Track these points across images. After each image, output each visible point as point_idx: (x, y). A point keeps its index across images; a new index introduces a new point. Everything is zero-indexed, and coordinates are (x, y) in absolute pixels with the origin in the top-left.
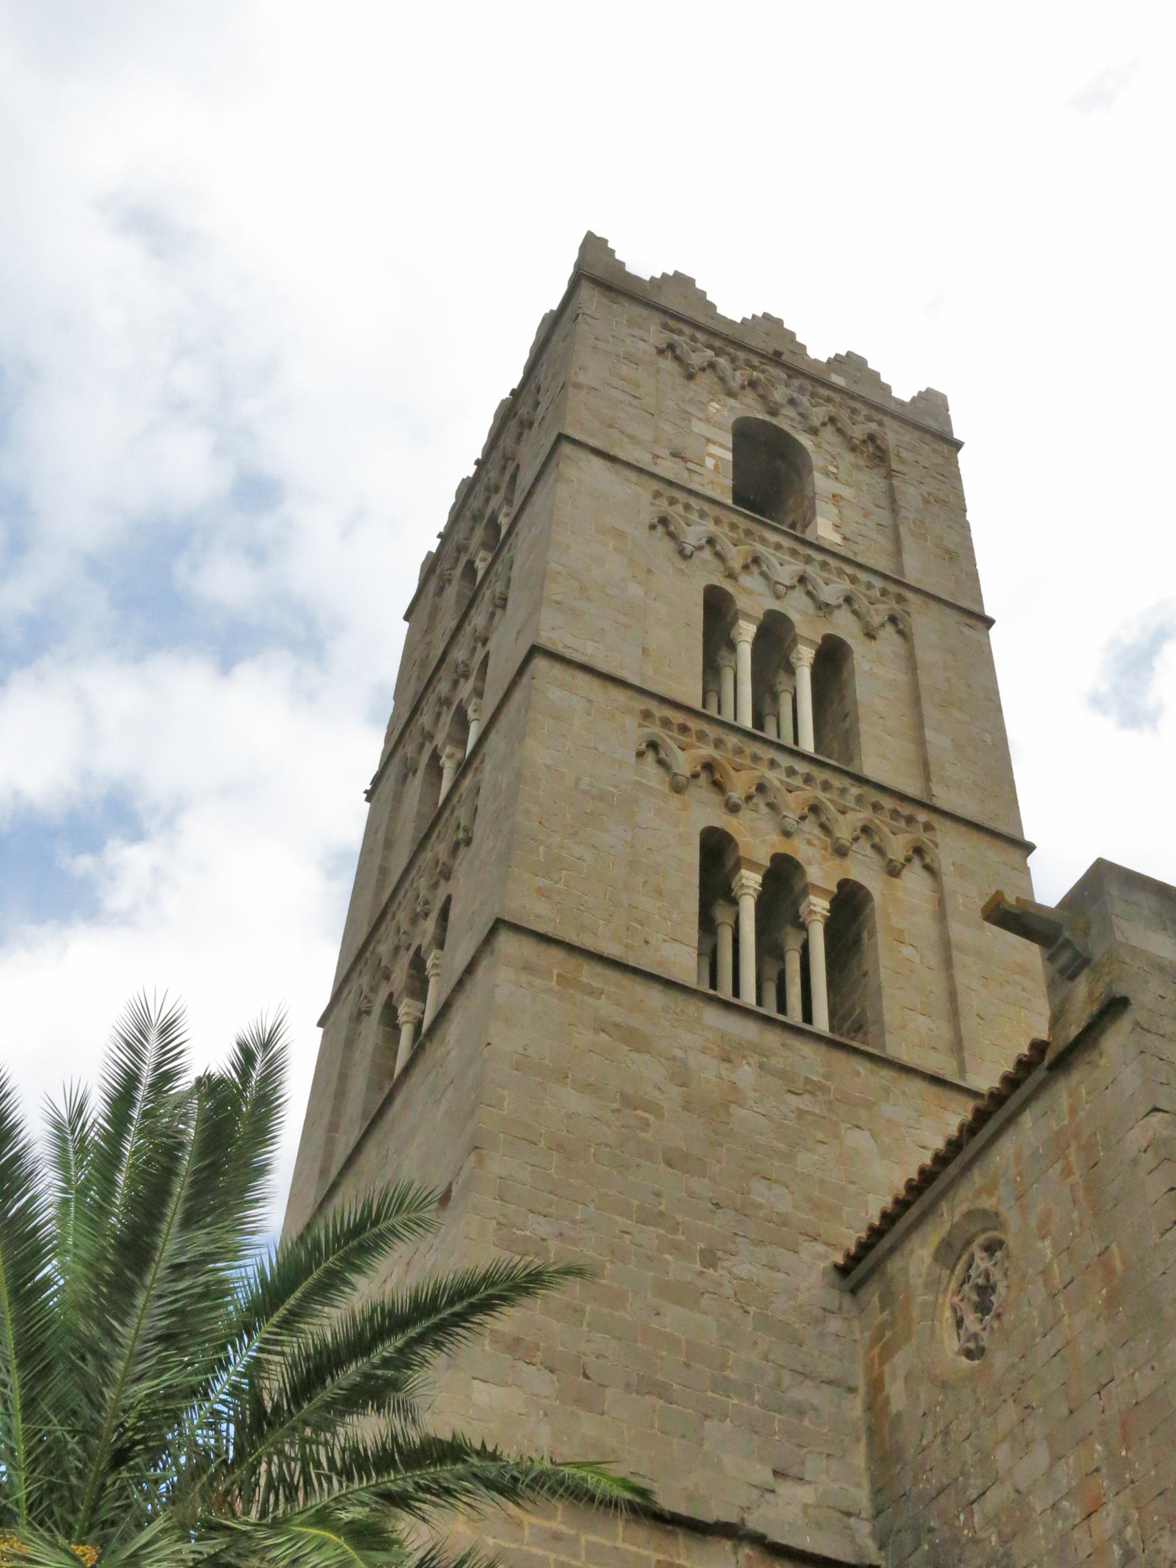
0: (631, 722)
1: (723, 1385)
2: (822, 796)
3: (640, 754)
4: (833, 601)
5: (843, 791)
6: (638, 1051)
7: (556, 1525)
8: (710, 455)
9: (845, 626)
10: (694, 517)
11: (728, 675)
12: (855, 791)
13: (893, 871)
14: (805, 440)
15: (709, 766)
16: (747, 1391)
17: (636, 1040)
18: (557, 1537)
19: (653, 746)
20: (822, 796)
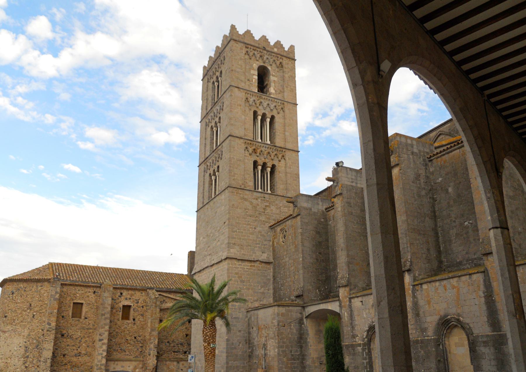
0: (243, 145)
1: (257, 244)
2: (270, 151)
3: (245, 150)
4: (272, 109)
5: (273, 149)
6: (246, 201)
7: (240, 263)
8: (254, 78)
9: (275, 113)
10: (251, 97)
11: (257, 124)
12: (275, 148)
13: (280, 161)
14: (269, 68)
15: (254, 150)
16: (259, 244)
17: (246, 200)
18: (240, 264)
19: (247, 148)
20: (270, 151)
